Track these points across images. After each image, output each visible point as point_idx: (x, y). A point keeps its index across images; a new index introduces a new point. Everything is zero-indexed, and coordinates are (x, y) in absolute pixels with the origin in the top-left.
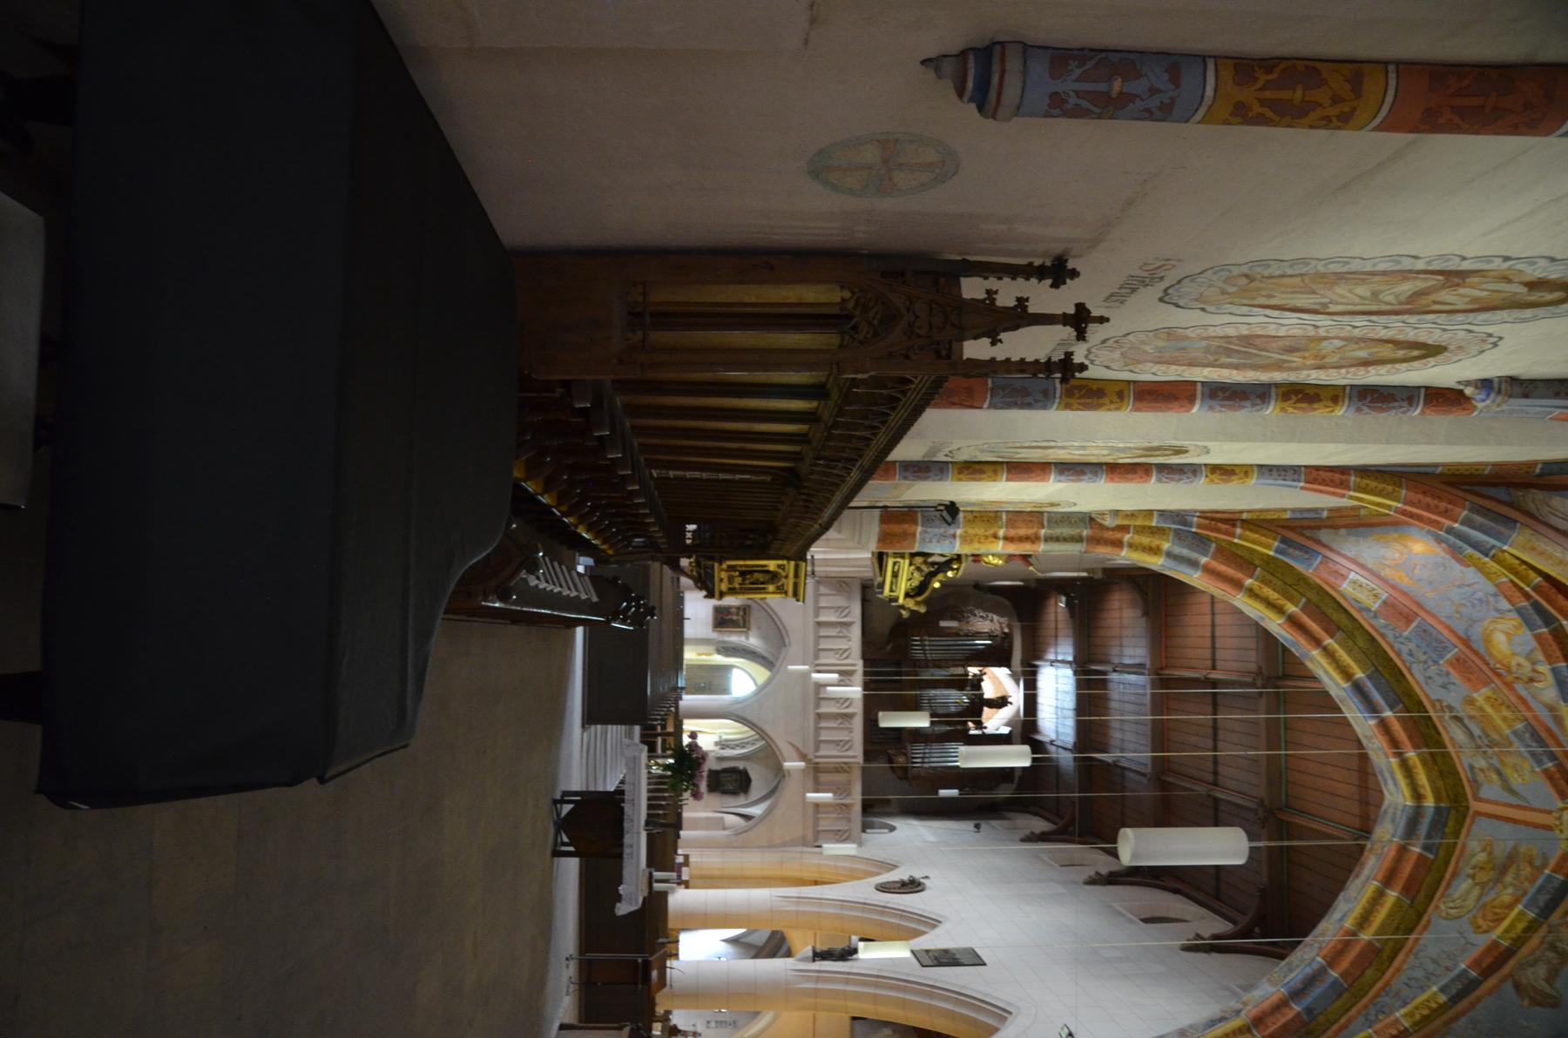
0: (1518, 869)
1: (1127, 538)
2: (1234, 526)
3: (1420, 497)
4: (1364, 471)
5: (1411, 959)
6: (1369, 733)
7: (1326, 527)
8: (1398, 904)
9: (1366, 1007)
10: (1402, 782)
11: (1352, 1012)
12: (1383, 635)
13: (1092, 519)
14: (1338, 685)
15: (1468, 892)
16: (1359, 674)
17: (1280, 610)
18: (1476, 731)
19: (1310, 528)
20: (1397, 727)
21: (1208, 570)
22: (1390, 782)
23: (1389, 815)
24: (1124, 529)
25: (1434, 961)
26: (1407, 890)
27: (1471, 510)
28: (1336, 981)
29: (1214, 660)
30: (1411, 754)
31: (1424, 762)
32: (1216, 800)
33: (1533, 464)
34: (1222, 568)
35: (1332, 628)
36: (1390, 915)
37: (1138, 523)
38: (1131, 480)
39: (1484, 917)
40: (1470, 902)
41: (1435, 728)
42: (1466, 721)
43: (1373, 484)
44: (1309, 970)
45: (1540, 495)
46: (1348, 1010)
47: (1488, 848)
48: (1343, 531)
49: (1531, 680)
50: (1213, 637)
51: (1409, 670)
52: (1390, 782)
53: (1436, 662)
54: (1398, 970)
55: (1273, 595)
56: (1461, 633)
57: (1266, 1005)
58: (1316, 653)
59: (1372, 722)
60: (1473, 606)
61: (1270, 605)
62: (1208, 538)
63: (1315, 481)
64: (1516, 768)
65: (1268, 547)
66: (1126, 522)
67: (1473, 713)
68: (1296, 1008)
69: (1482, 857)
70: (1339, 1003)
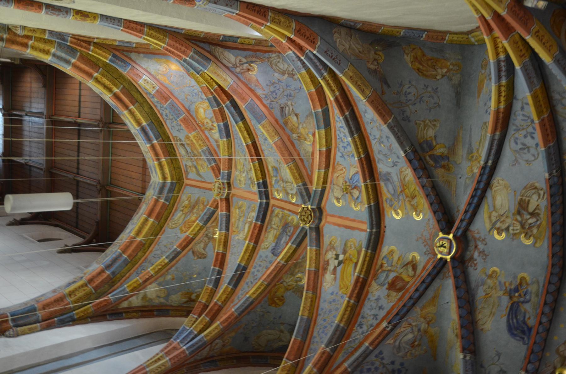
1: (31, 43)
2: (90, 45)
3: (174, 43)
4: (151, 27)
5: (156, 246)
6: (147, 150)
7: (135, 52)
8: (153, 224)
9: (137, 268)
10: (159, 172)
11: (131, 271)
12: (155, 106)
13: (9, 29)
14: (135, 128)
15: (180, 217)
16: (144, 124)
17: (110, 90)
18: (189, 150)
19: (127, 51)
20: (158, 148)
21: (75, 66)
22: (154, 172)
23: (152, 187)
24: (29, 37)
25: (165, 246)
26: (157, 218)
27: (194, 52)
28: (126, 259)
29: (79, 113)
30: (163, 160)
31: (168, 163)
32: (78, 182)
33: (219, 35)
34: (83, 66)
35: (134, 101)
36: (149, 229)
37: (38, 35)
38: (31, 10)
40: (180, 221)
41: (174, 149)
42: (186, 146)
43: (154, 34)
44: (114, 256)
45: (220, 50)
46: (130, 270)
47: (189, 199)
48: (142, 55)
49: (211, 129)
50: (80, 101)
51: (165, 122)
52: (154, 172)
53: (176, 120)
54: (151, 251)
55: (107, 83)
56: (187, 107)
57: (94, 273)
58: (126, 112)
59: (148, 145)
60: (193, 96)
61: (105, 87)
62: (76, 49)
63: (128, 28)
64: (202, 166)
65: (106, 58)
66: (30, 34)
67: (189, 142)
68: (108, 273)
69: (187, 202)
70: (126, 268)
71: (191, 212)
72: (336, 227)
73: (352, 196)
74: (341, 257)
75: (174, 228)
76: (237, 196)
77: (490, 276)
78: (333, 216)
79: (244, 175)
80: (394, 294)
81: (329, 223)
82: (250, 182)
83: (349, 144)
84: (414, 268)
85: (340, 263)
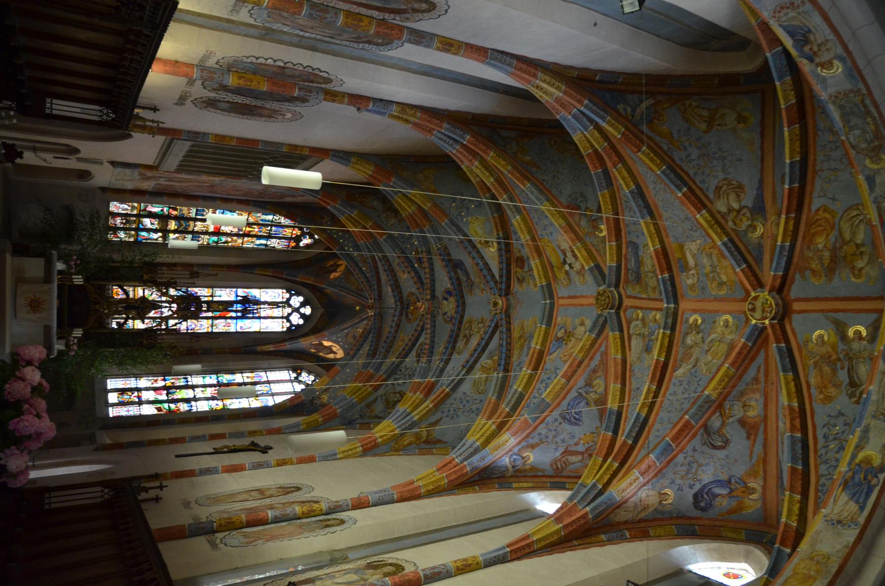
0: (823, 265)
15: (854, 234)
18: (843, 376)
39: (827, 220)
42: (847, 381)
69: (860, 264)
71: (834, 251)
72: (584, 294)
73: (566, 330)
74: (567, 267)
75: (850, 208)
76: (736, 300)
77: (483, 290)
78: (589, 305)
79: (713, 336)
80: (518, 255)
81: (591, 297)
82: (703, 327)
83: (543, 381)
84: (518, 279)
85: (565, 262)
